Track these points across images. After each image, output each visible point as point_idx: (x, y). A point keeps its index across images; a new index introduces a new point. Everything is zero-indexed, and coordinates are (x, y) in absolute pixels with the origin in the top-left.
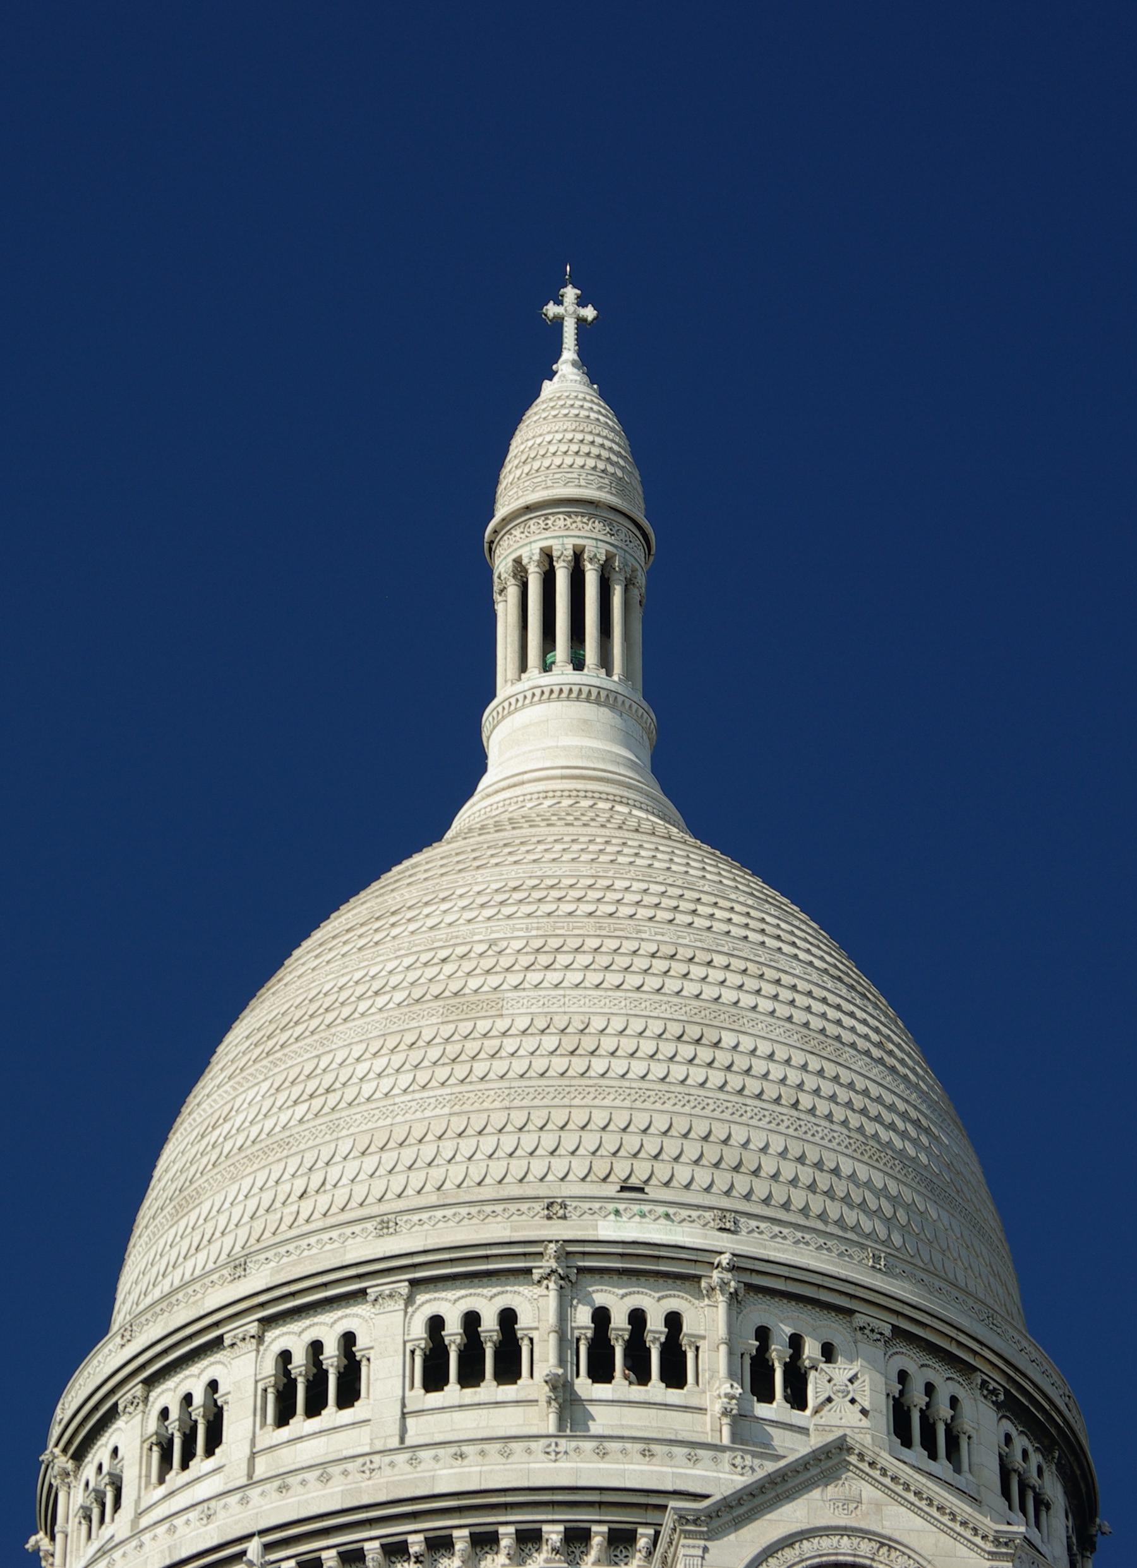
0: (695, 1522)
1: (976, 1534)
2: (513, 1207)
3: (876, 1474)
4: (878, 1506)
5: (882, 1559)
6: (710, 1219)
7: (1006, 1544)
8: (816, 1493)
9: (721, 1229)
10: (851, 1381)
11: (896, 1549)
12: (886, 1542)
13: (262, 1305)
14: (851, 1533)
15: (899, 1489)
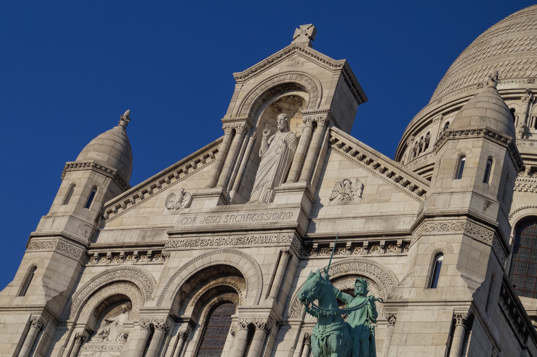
0: (240, 78)
1: (330, 66)
2: (469, 88)
3: (304, 53)
4: (303, 64)
5: (299, 79)
6: (526, 81)
7: (339, 66)
8: (284, 63)
9: (529, 83)
10: (308, 29)
11: (304, 75)
12: (301, 73)
13: (413, 131)
14: (290, 73)
15: (310, 56)
